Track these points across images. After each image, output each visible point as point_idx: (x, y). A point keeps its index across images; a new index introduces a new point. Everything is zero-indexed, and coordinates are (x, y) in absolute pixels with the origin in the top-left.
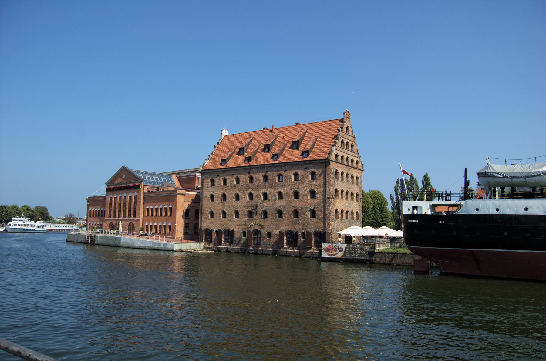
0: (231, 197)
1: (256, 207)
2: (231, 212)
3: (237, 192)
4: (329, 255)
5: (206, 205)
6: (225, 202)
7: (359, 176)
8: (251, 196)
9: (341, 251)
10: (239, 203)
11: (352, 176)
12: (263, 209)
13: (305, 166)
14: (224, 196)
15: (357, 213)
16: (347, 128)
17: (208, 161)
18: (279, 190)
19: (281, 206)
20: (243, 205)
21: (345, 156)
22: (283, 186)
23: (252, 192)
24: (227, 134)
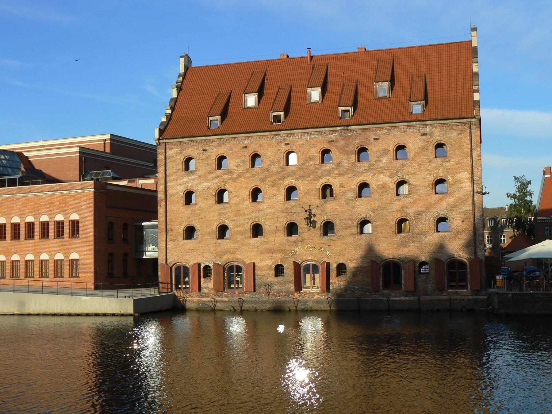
2: (240, 226)
5: (175, 213)
13: (422, 130)
19: (369, 210)
20: (273, 210)
22: (371, 170)
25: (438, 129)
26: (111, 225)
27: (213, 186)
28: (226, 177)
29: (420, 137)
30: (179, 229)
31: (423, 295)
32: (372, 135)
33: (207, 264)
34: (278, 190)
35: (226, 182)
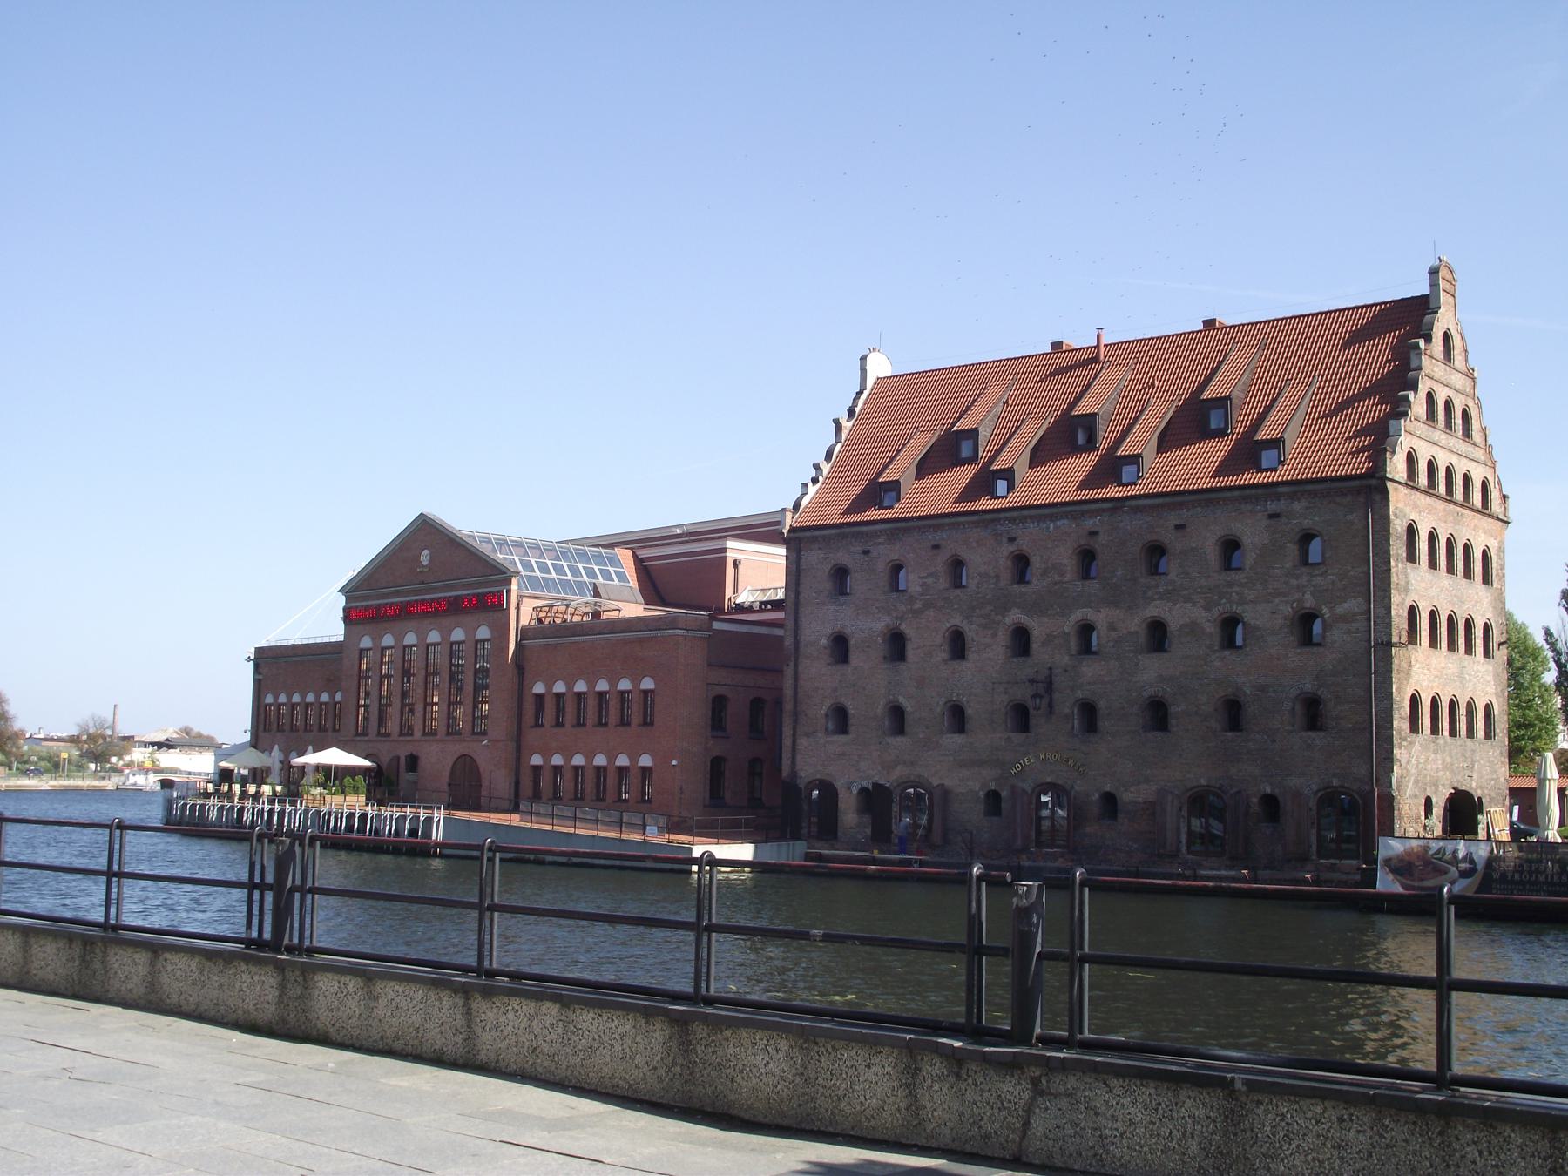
0: (927, 638)
1: (1049, 685)
3: (957, 620)
4: (1404, 886)
5: (818, 680)
6: (902, 666)
7: (1493, 546)
8: (1021, 641)
9: (1464, 874)
10: (967, 668)
11: (1467, 549)
12: (1079, 694)
13: (1272, 507)
14: (897, 645)
15: (1488, 709)
16: (1447, 337)
17: (812, 489)
18: (1152, 611)
20: (985, 674)
21: (1442, 461)
23: (1025, 619)
24: (887, 371)
25: (1304, 503)
26: (718, 704)
27: (879, 624)
28: (902, 607)
29: (1266, 522)
30: (818, 710)
31: (1266, 868)
32: (1174, 519)
33: (865, 784)
34: (994, 635)
35: (901, 618)
